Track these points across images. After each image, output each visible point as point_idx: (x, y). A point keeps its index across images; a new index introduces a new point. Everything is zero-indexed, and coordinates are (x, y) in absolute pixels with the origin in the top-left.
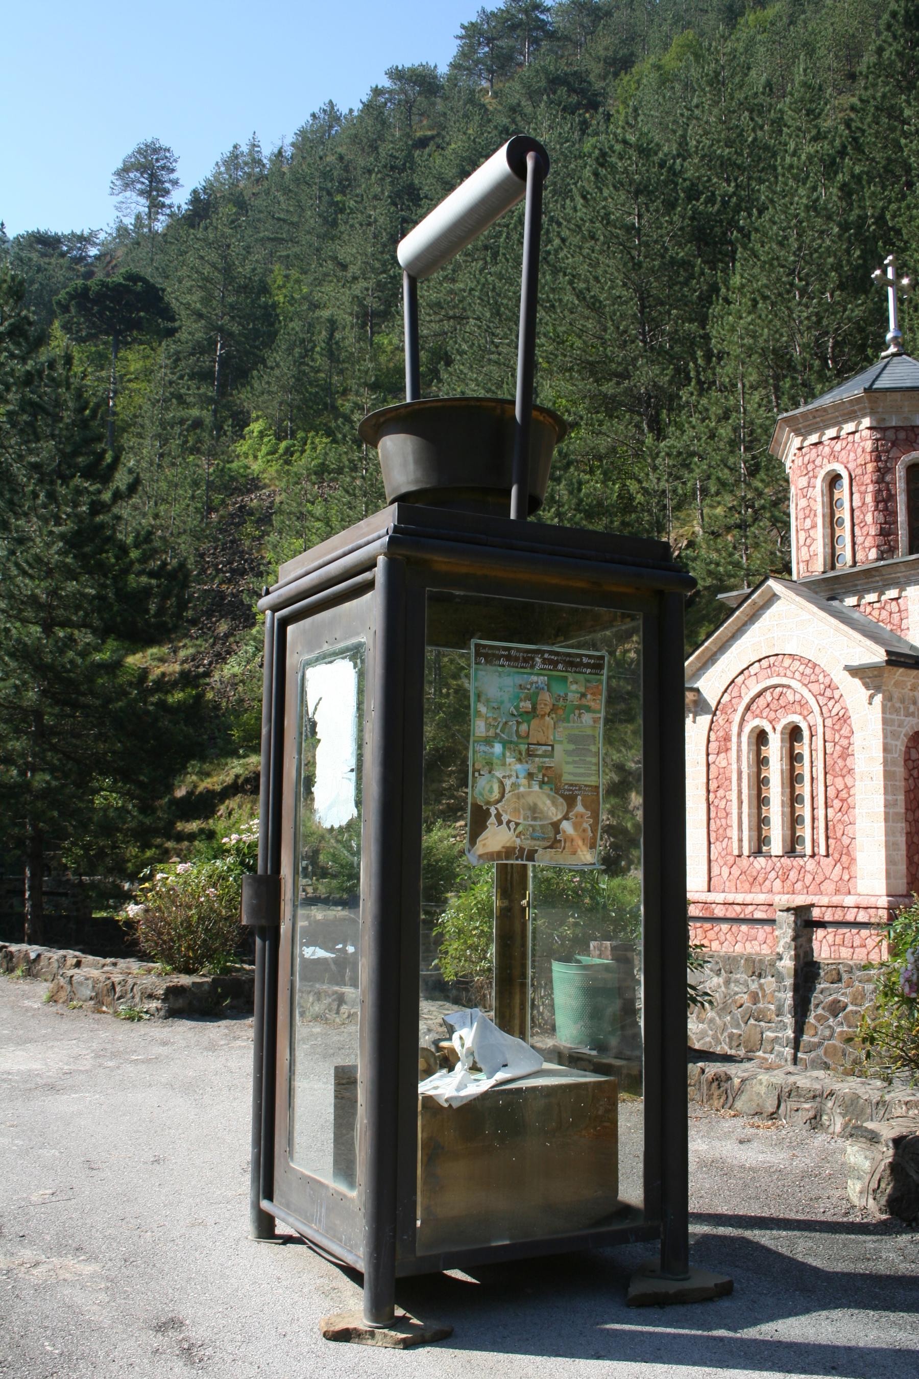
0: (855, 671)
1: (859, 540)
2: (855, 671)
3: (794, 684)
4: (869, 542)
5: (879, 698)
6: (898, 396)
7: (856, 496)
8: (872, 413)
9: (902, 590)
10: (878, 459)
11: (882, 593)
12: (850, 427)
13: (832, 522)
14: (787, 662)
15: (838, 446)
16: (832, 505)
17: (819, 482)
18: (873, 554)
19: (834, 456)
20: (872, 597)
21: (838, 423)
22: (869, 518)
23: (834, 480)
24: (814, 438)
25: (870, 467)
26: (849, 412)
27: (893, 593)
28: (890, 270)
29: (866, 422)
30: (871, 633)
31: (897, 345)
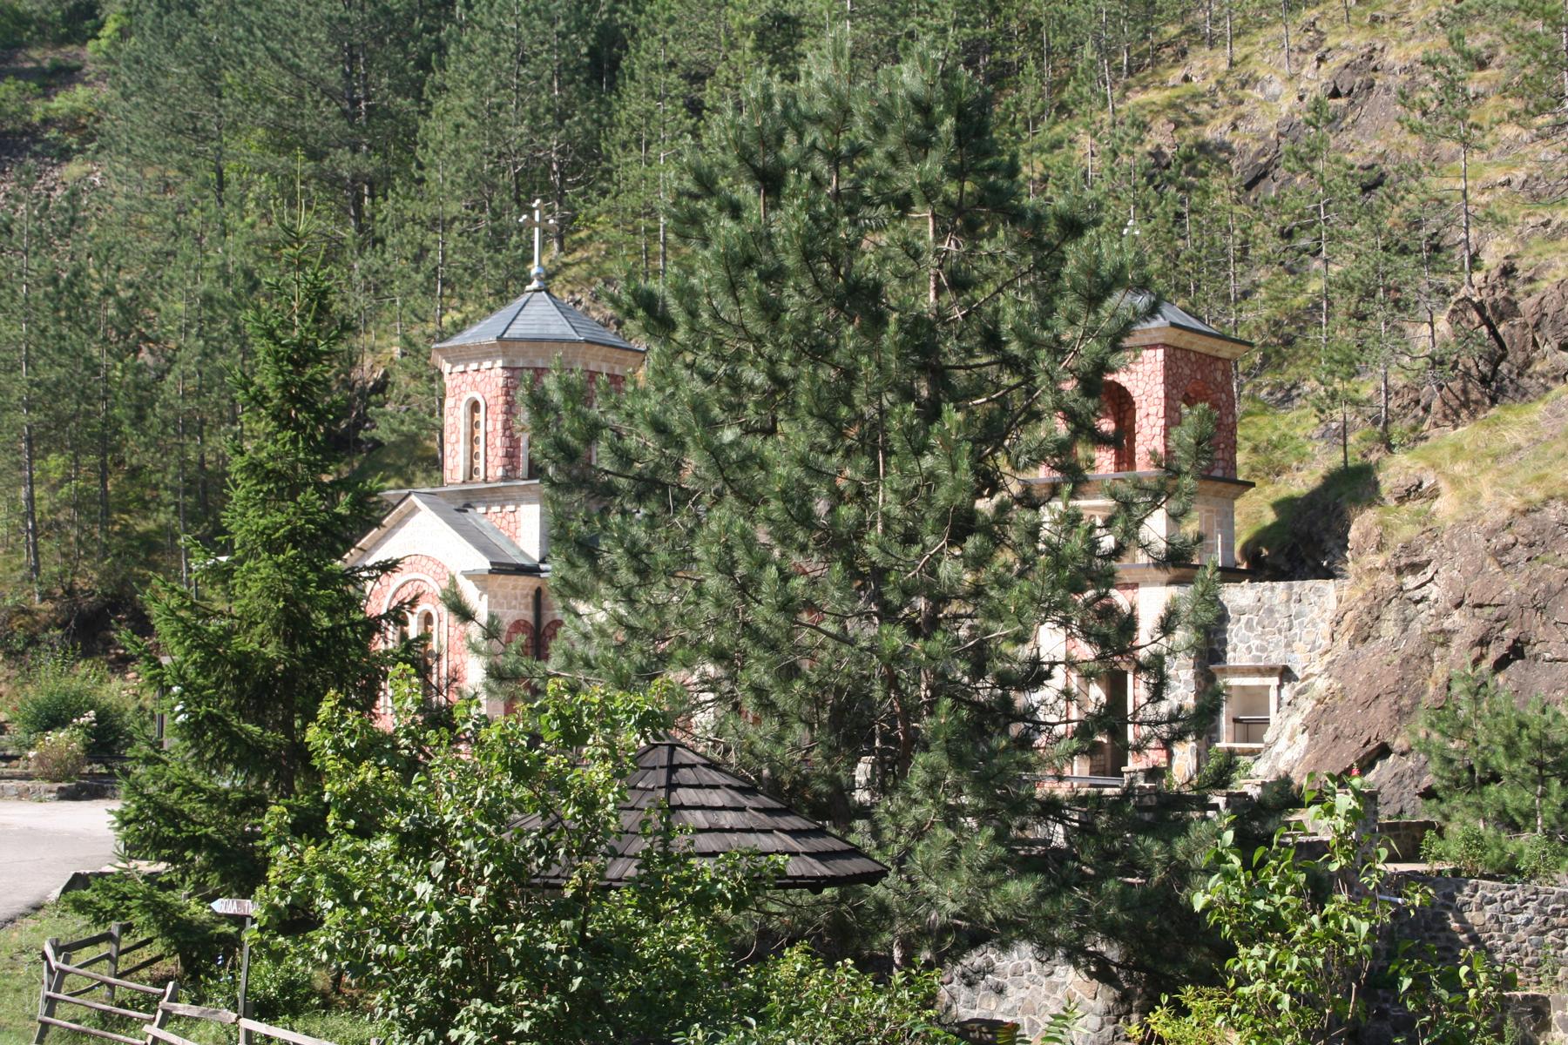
0: (469, 575)
1: (490, 459)
2: (469, 575)
3: (429, 579)
4: (498, 461)
5: (485, 597)
6: (524, 345)
7: (490, 422)
8: (505, 355)
9: (517, 506)
10: (507, 394)
11: (503, 507)
12: (487, 364)
13: (473, 440)
14: (424, 561)
15: (479, 377)
16: (474, 425)
17: (462, 405)
18: (500, 472)
19: (474, 385)
20: (496, 509)
21: (480, 360)
22: (498, 443)
23: (475, 406)
24: (461, 368)
25: (501, 400)
26: (484, 353)
27: (511, 508)
28: (537, 213)
29: (500, 363)
30: (484, 547)
31: (540, 280)
